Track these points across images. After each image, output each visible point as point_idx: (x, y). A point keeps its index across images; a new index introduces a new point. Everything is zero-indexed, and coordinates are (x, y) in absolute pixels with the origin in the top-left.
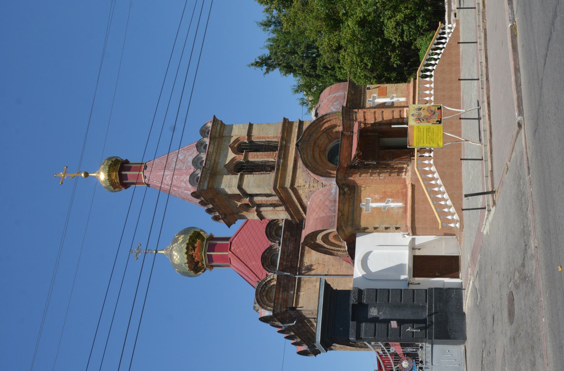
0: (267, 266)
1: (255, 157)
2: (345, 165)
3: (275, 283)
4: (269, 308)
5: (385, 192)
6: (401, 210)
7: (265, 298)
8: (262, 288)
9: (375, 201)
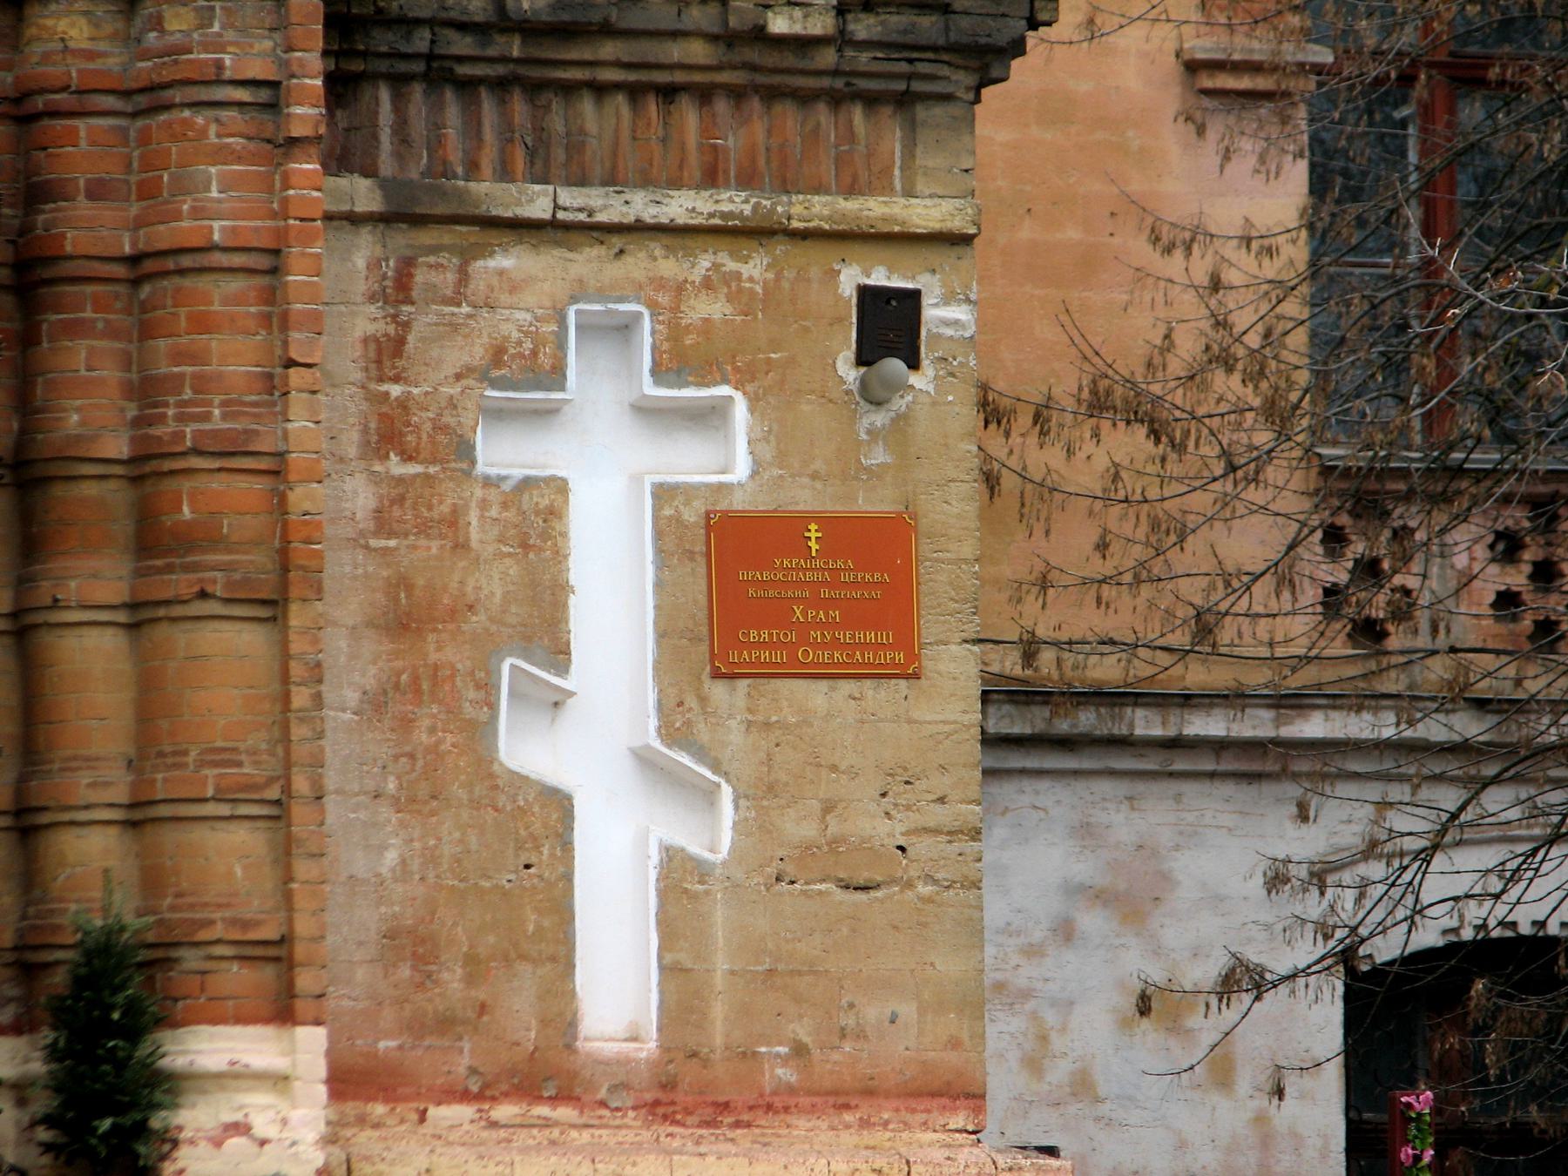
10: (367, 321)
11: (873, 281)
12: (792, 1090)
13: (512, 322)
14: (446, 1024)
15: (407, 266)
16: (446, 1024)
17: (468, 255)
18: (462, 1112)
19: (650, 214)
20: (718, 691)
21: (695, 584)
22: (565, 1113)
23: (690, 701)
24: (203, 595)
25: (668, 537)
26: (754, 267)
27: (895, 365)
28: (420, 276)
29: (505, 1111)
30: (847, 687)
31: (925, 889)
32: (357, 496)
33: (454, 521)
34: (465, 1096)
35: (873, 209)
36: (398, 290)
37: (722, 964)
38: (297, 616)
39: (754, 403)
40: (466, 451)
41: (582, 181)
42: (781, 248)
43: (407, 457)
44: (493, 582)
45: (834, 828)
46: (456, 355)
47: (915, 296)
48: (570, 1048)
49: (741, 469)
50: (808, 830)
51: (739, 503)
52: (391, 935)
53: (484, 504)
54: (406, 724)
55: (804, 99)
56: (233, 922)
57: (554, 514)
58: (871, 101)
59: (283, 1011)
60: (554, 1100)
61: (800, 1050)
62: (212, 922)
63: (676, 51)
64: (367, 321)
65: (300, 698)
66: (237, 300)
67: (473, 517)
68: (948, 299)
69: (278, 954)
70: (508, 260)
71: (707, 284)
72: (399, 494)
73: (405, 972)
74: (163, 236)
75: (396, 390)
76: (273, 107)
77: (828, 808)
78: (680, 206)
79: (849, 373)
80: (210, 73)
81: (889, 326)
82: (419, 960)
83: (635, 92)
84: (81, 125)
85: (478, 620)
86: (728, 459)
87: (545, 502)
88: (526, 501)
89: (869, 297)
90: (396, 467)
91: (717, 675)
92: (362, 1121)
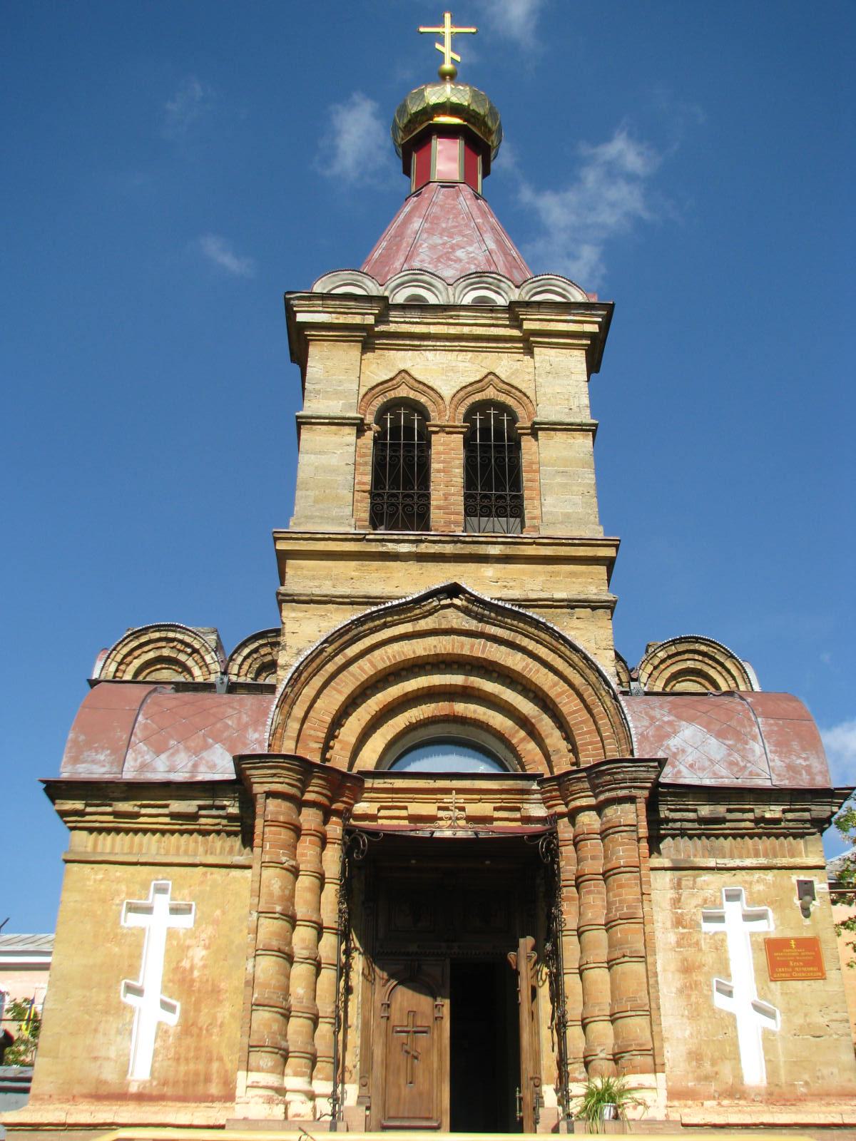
0: (256, 651)
1: (447, 462)
2: (361, 808)
3: (200, 679)
4: (113, 667)
5: (215, 991)
6: (109, 1074)
7: (151, 655)
8: (182, 642)
9: (177, 946)
10: (671, 894)
11: (802, 878)
12: (806, 1095)
13: (708, 893)
14: (707, 1078)
15: (679, 881)
16: (707, 1078)
17: (695, 877)
18: (714, 1103)
19: (741, 864)
20: (772, 985)
21: (763, 957)
22: (742, 1102)
23: (765, 988)
24: (624, 956)
25: (754, 945)
26: (770, 876)
27: (808, 898)
28: (684, 883)
29: (725, 1102)
30: (807, 982)
31: (835, 1036)
32: (672, 938)
33: (697, 943)
34: (714, 1098)
35: (798, 861)
36: (678, 886)
37: (782, 1059)
38: (650, 960)
39: (773, 910)
40: (699, 925)
41: (724, 857)
42: (776, 871)
43: (684, 928)
44: (709, 958)
45: (808, 1020)
46: (694, 902)
47: (811, 882)
48: (742, 1084)
49: (772, 928)
50: (801, 1021)
51: (773, 936)
52: (690, 1053)
53: (705, 939)
54: (689, 996)
55: (777, 836)
56: (638, 1045)
57: (723, 941)
58: (795, 836)
59: (656, 1069)
60: (739, 1099)
61: (807, 1083)
62: (631, 1045)
63: (743, 825)
64: (671, 894)
65: (652, 981)
66: (629, 879)
67: (703, 942)
68: (821, 882)
69: (652, 1052)
70: (706, 877)
71: (758, 881)
72: (683, 937)
73: (694, 1063)
74: (609, 866)
75: (679, 911)
76: (636, 831)
77: (806, 1015)
78: (748, 862)
79: (798, 903)
80: (618, 824)
81: (806, 889)
82: (697, 1060)
83: (735, 836)
84: (588, 842)
85: (706, 969)
86: (769, 927)
87: (721, 938)
88: (716, 938)
89: (801, 884)
90: (681, 930)
91: (771, 981)
92: (685, 1106)
